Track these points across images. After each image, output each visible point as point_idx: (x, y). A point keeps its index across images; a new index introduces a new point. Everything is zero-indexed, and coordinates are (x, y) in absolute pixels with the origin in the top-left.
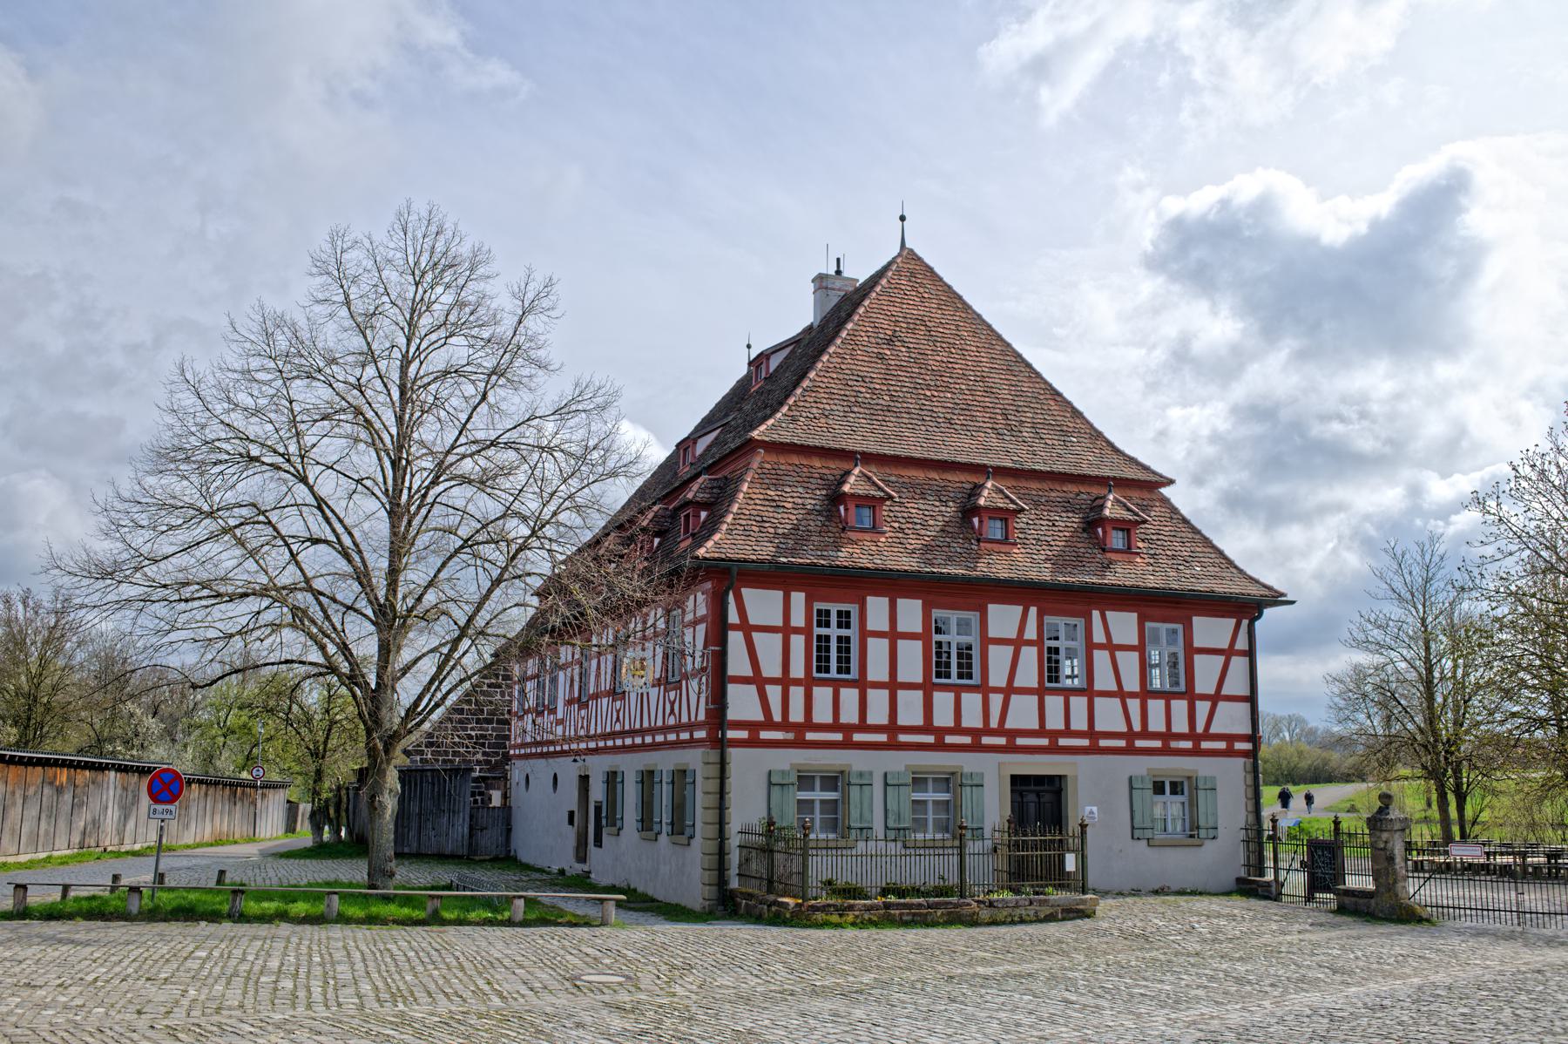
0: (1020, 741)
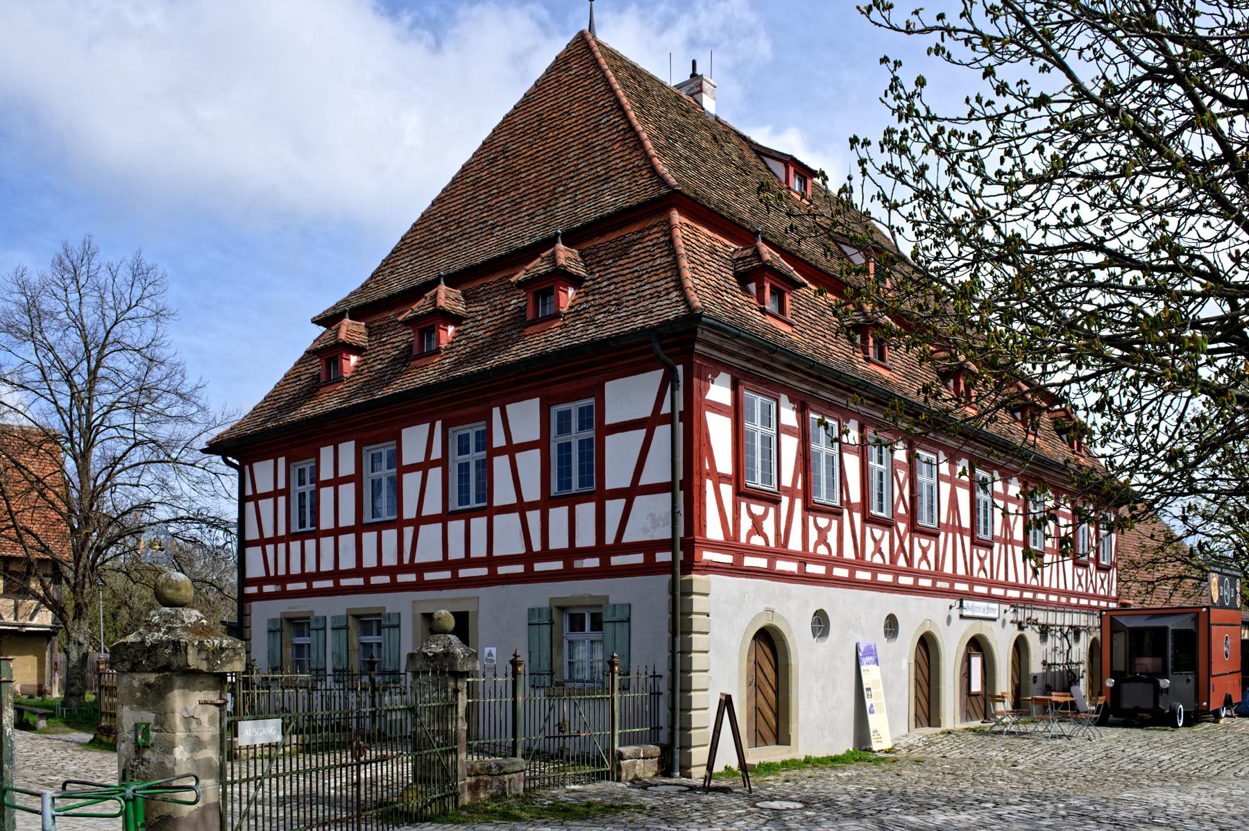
0: (428, 576)
